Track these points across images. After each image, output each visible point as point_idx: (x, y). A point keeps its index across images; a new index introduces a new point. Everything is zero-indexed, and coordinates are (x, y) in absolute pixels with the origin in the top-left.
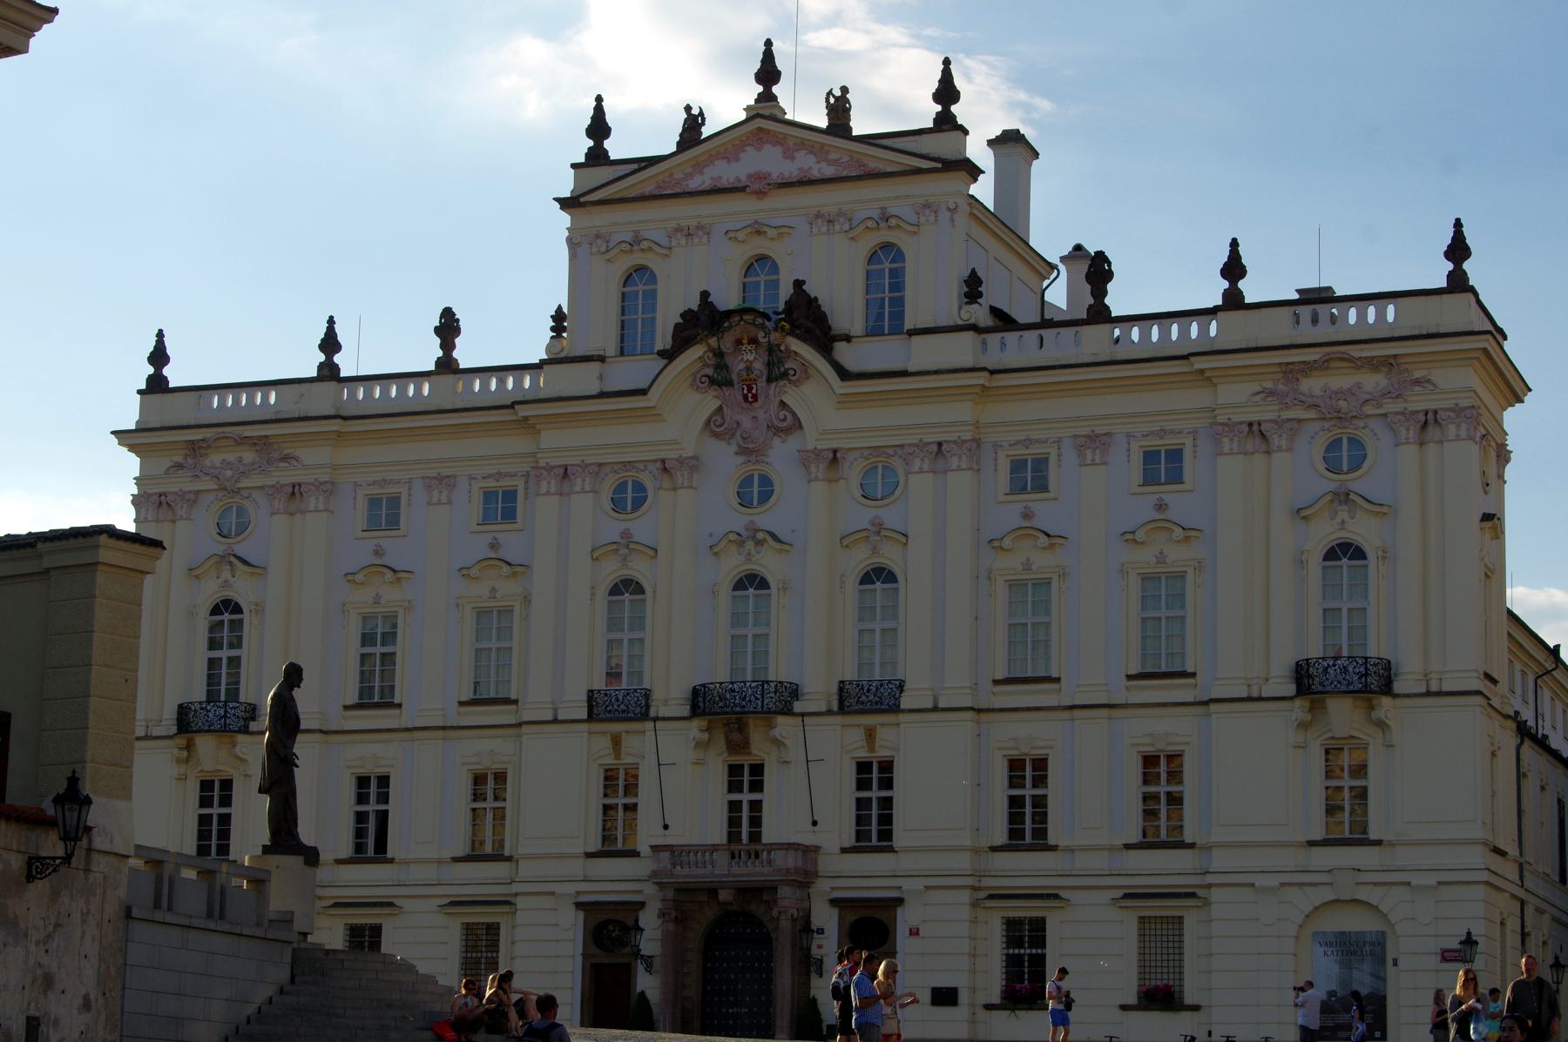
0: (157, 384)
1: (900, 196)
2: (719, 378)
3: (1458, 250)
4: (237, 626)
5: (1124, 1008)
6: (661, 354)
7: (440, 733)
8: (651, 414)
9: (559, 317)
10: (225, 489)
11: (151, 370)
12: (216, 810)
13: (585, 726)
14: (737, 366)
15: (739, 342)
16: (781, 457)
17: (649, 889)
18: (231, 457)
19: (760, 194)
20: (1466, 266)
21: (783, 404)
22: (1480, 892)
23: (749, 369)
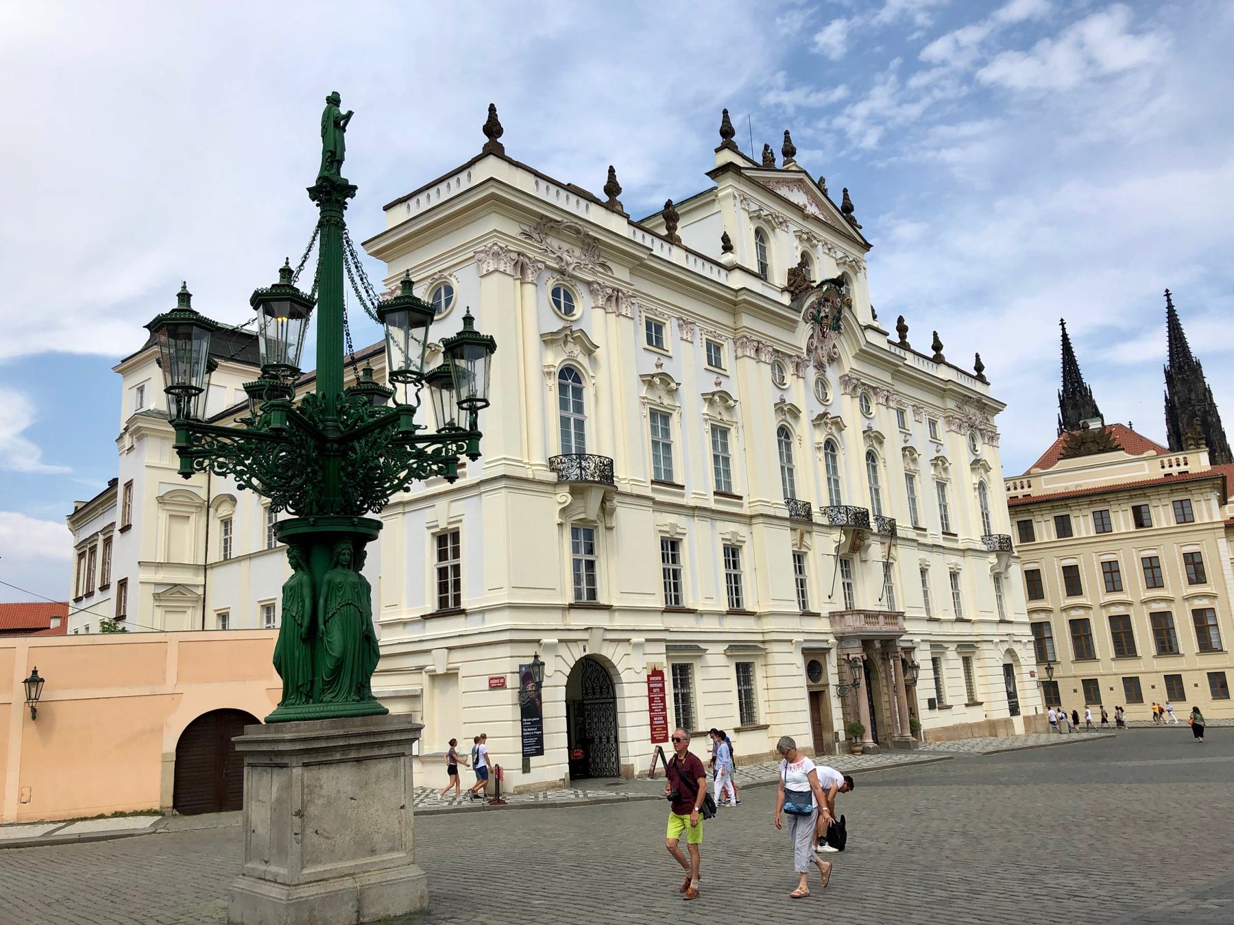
0: (494, 149)
1: (854, 252)
2: (816, 320)
3: (979, 367)
4: (578, 393)
5: (967, 705)
6: (783, 290)
7: (709, 514)
8: (791, 325)
9: (725, 239)
10: (562, 272)
11: (486, 140)
12: (584, 557)
13: (788, 523)
14: (823, 314)
15: (827, 300)
16: (832, 374)
17: (832, 640)
18: (565, 246)
19: (806, 217)
20: (983, 373)
21: (834, 346)
22: (1031, 646)
23: (827, 317)
